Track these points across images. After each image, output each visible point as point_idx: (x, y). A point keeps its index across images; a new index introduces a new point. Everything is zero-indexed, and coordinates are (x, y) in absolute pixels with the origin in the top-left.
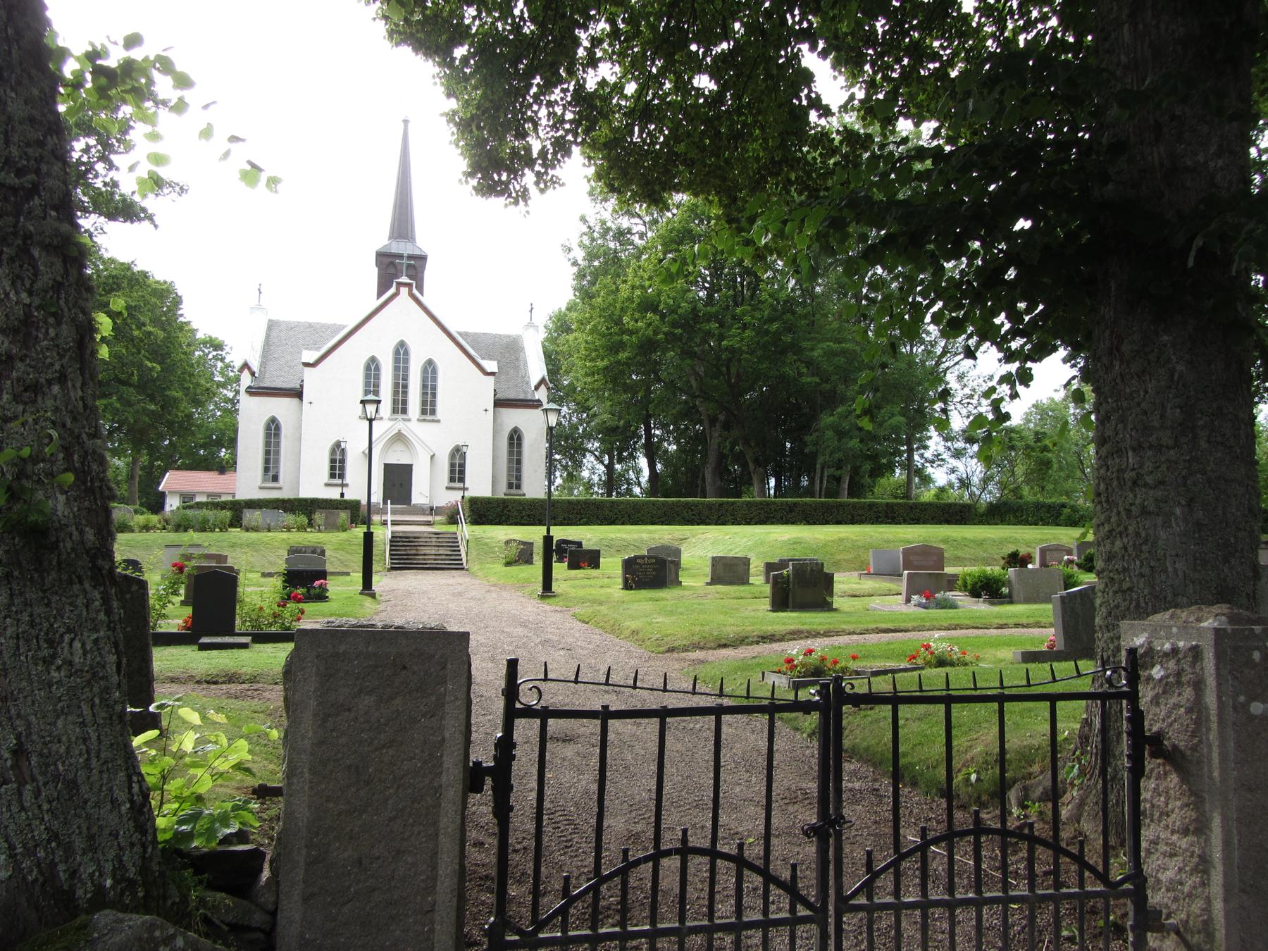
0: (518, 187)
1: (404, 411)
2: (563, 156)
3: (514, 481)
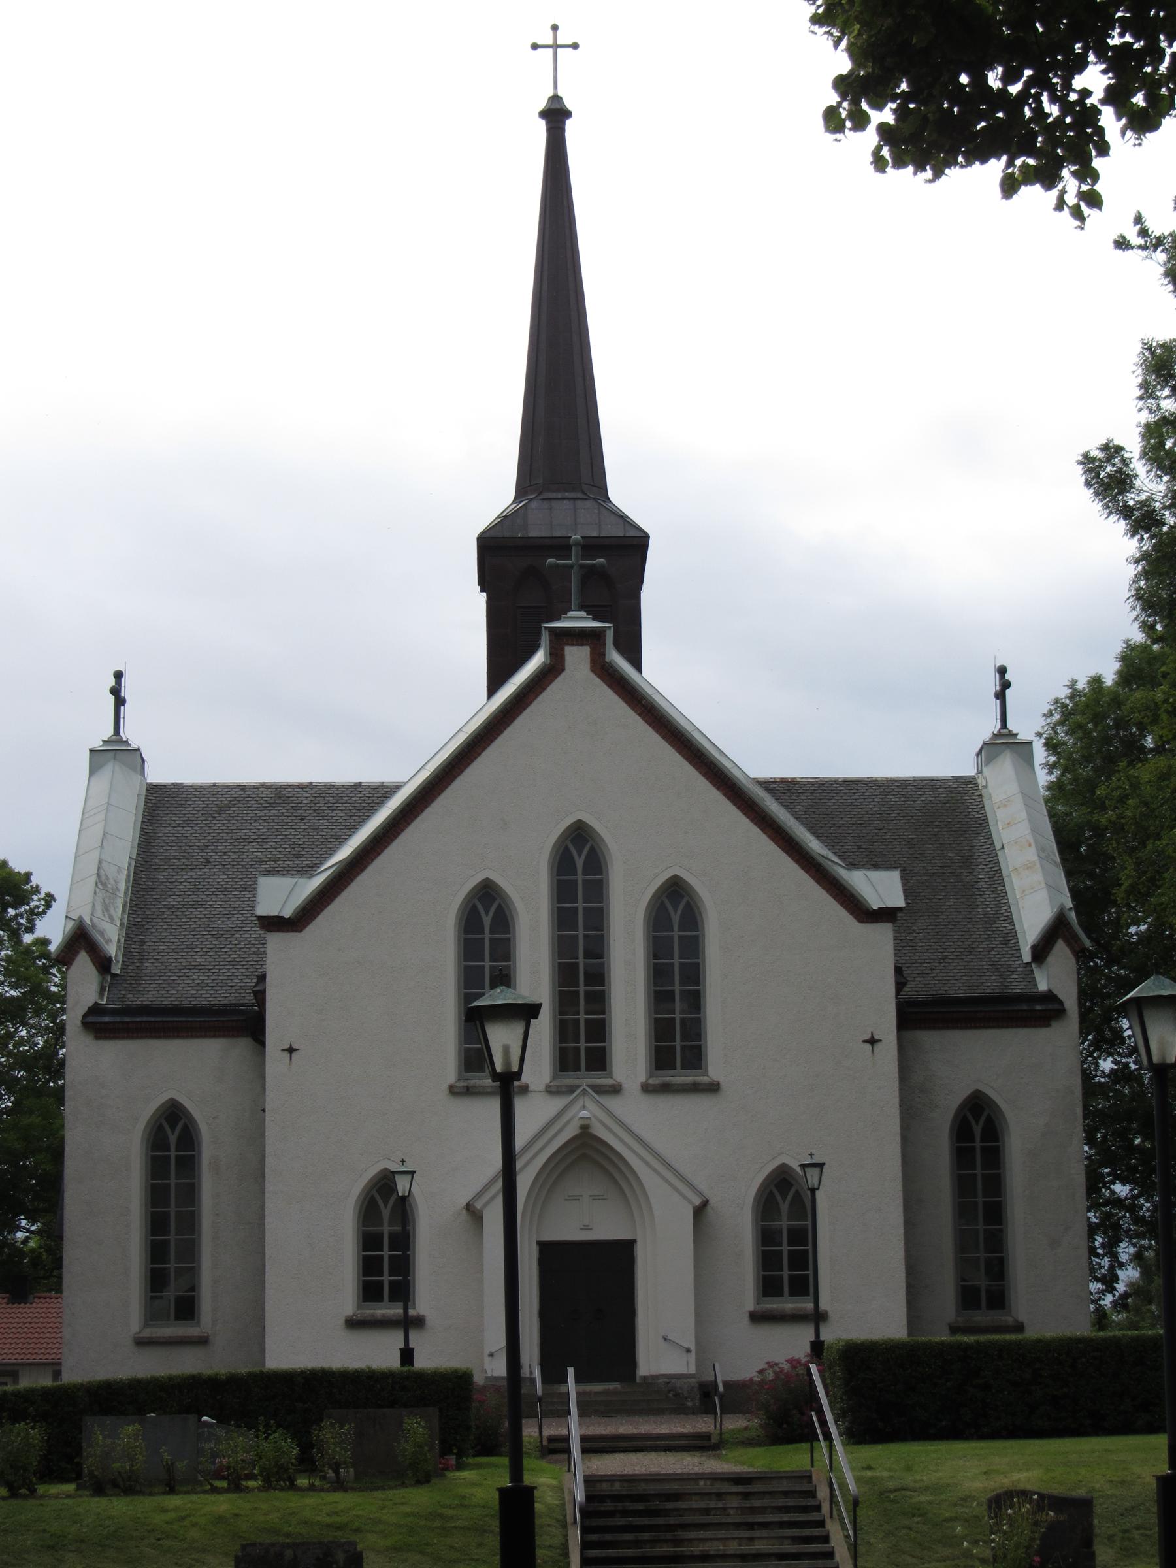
0: (1052, 110)
1: (599, 1061)
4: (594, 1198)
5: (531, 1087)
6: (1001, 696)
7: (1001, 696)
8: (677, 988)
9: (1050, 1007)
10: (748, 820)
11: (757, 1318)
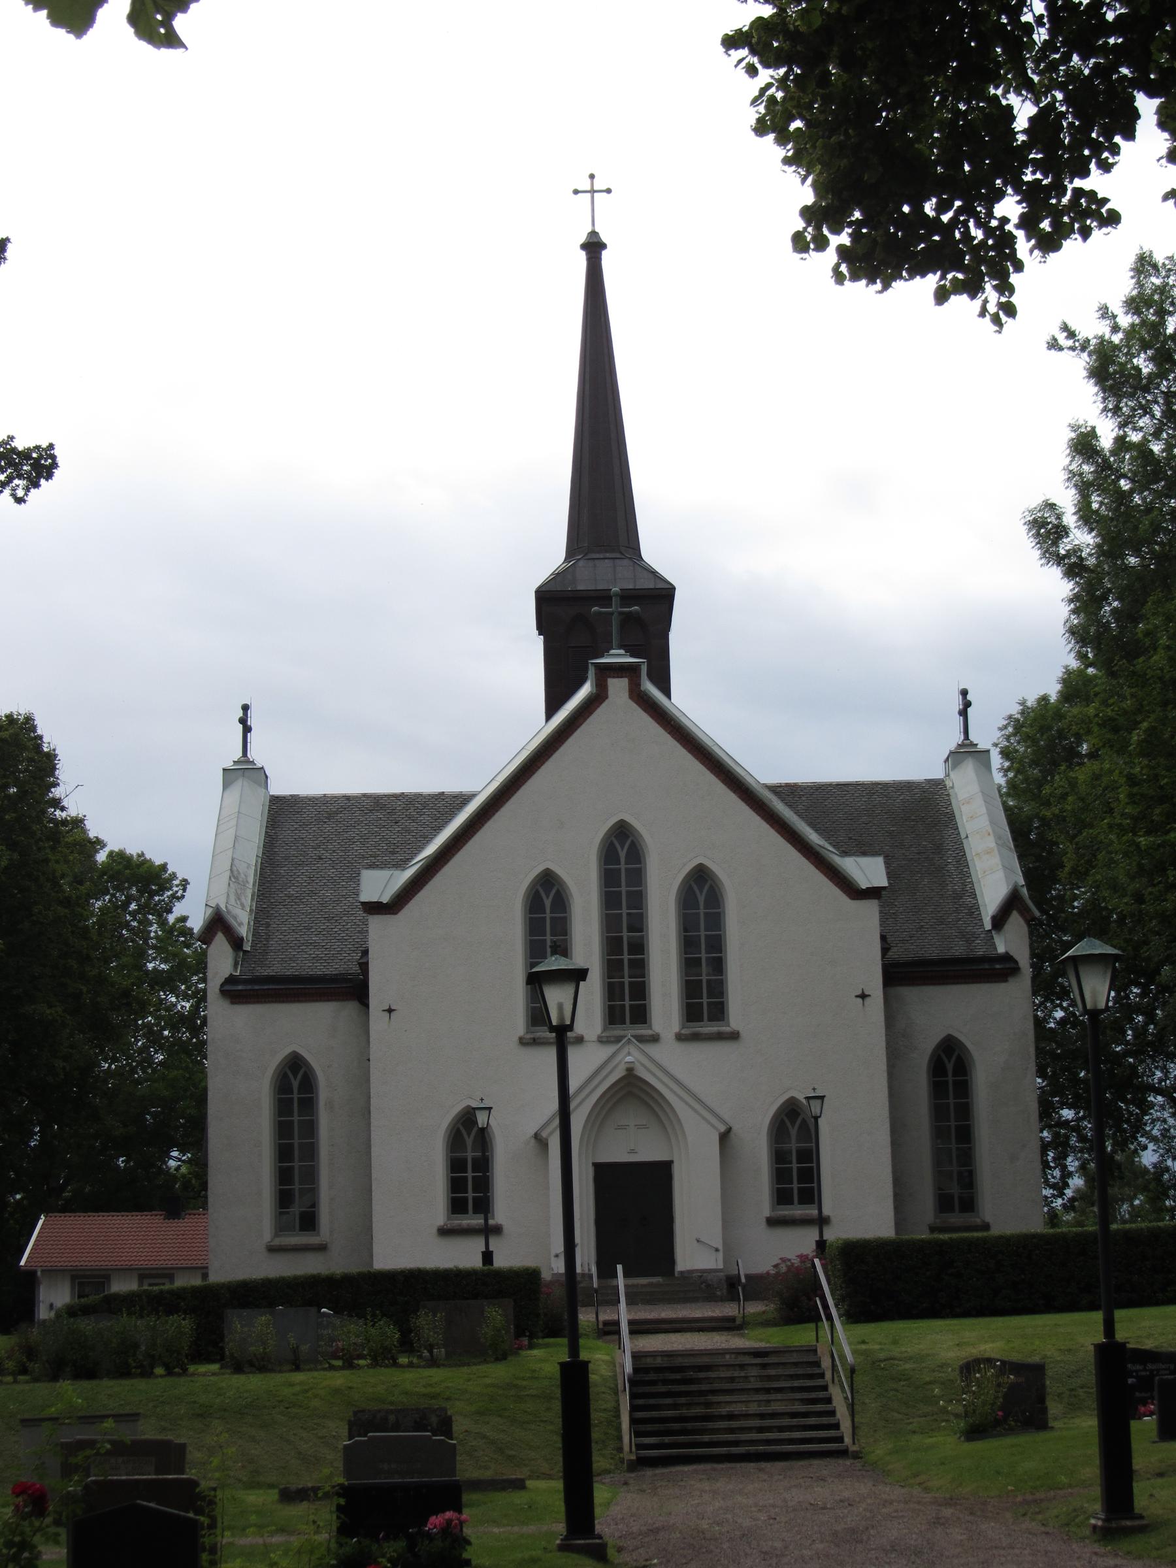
0: (978, 234)
1: (641, 1015)
2: (1109, 134)
3: (955, 1190)
4: (639, 1127)
5: (586, 1038)
6: (964, 713)
7: (964, 713)
8: (703, 955)
9: (1008, 966)
10: (758, 818)
11: (772, 1222)
